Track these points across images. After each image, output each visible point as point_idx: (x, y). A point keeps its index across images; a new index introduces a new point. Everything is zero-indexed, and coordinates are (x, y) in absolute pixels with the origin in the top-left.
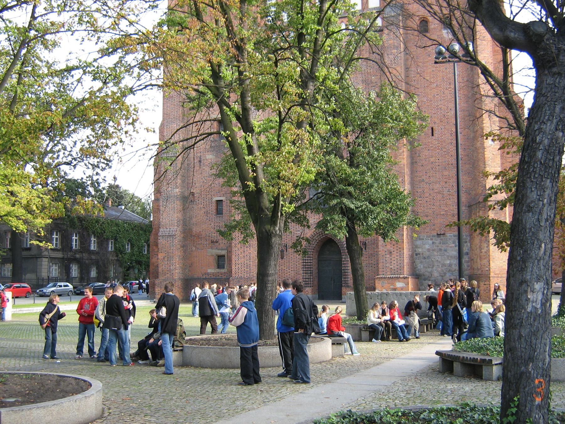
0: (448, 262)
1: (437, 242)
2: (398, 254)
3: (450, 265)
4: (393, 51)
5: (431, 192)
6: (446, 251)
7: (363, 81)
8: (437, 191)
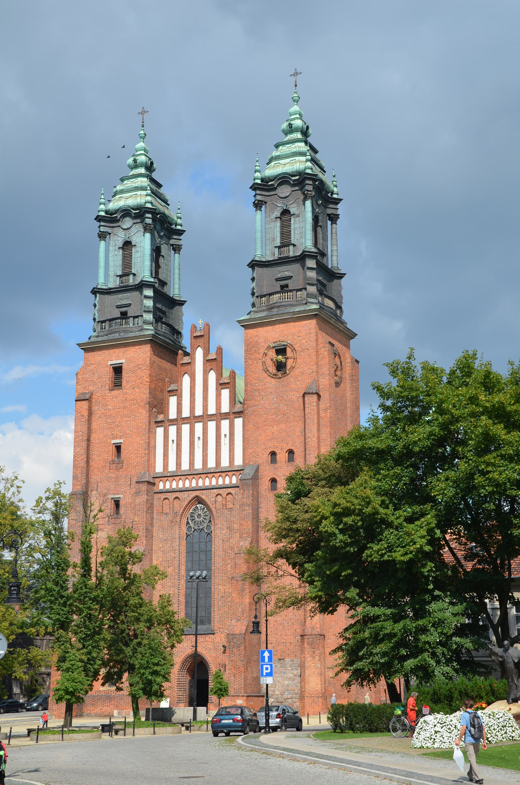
0: (287, 682)
1: (279, 665)
2: (240, 677)
3: (288, 686)
4: (246, 508)
5: (275, 624)
6: (285, 673)
7: (228, 528)
8: (279, 623)
